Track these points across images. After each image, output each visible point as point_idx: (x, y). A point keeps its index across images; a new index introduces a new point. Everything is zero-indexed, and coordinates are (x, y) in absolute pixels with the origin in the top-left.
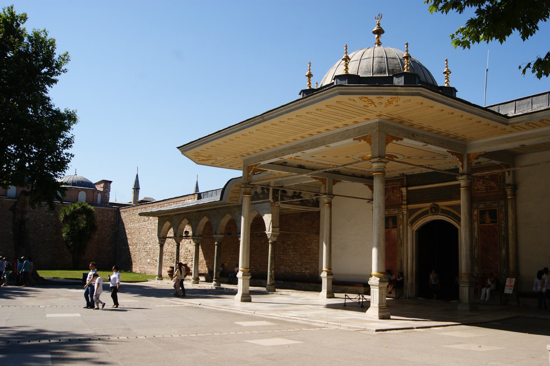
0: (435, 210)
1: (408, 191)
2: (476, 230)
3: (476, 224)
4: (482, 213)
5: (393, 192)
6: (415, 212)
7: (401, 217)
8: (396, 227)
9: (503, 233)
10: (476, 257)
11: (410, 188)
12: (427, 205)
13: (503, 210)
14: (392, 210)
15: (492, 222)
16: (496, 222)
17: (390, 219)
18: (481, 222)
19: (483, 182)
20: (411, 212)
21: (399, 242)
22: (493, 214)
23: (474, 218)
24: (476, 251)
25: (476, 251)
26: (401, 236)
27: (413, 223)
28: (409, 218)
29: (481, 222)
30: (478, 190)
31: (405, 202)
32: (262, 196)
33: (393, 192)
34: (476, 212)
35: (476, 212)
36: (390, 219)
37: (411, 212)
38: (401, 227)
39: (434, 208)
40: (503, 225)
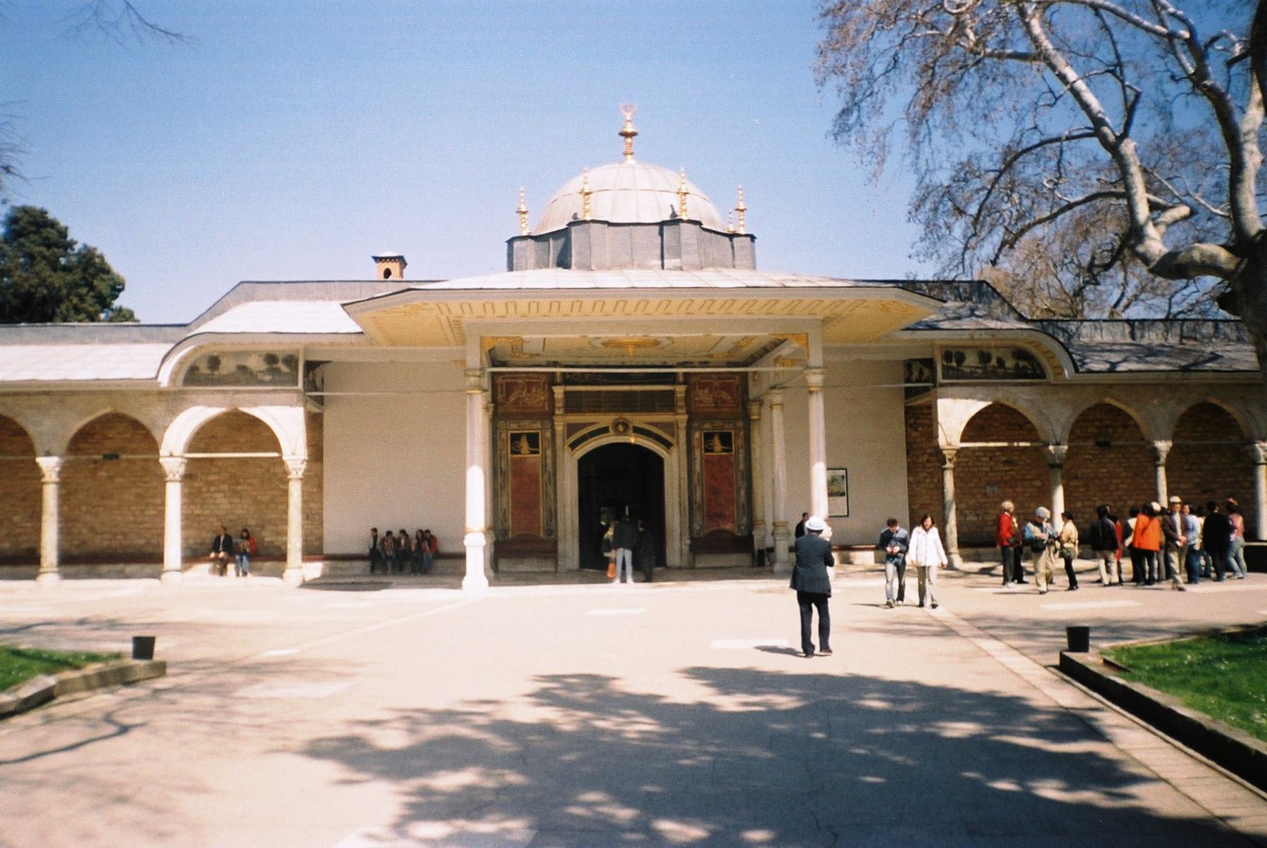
1: (566, 393)
2: (698, 460)
3: (697, 453)
4: (708, 437)
5: (529, 391)
7: (548, 435)
11: (570, 388)
12: (605, 419)
14: (526, 423)
15: (724, 451)
17: (524, 439)
18: (707, 450)
19: (710, 391)
20: (571, 429)
21: (546, 478)
22: (726, 440)
23: (696, 443)
24: (698, 494)
26: (549, 468)
27: (573, 446)
28: (569, 436)
30: (701, 402)
32: (267, 378)
33: (529, 391)
34: (697, 435)
36: (524, 439)
37: (571, 429)
38: (549, 452)
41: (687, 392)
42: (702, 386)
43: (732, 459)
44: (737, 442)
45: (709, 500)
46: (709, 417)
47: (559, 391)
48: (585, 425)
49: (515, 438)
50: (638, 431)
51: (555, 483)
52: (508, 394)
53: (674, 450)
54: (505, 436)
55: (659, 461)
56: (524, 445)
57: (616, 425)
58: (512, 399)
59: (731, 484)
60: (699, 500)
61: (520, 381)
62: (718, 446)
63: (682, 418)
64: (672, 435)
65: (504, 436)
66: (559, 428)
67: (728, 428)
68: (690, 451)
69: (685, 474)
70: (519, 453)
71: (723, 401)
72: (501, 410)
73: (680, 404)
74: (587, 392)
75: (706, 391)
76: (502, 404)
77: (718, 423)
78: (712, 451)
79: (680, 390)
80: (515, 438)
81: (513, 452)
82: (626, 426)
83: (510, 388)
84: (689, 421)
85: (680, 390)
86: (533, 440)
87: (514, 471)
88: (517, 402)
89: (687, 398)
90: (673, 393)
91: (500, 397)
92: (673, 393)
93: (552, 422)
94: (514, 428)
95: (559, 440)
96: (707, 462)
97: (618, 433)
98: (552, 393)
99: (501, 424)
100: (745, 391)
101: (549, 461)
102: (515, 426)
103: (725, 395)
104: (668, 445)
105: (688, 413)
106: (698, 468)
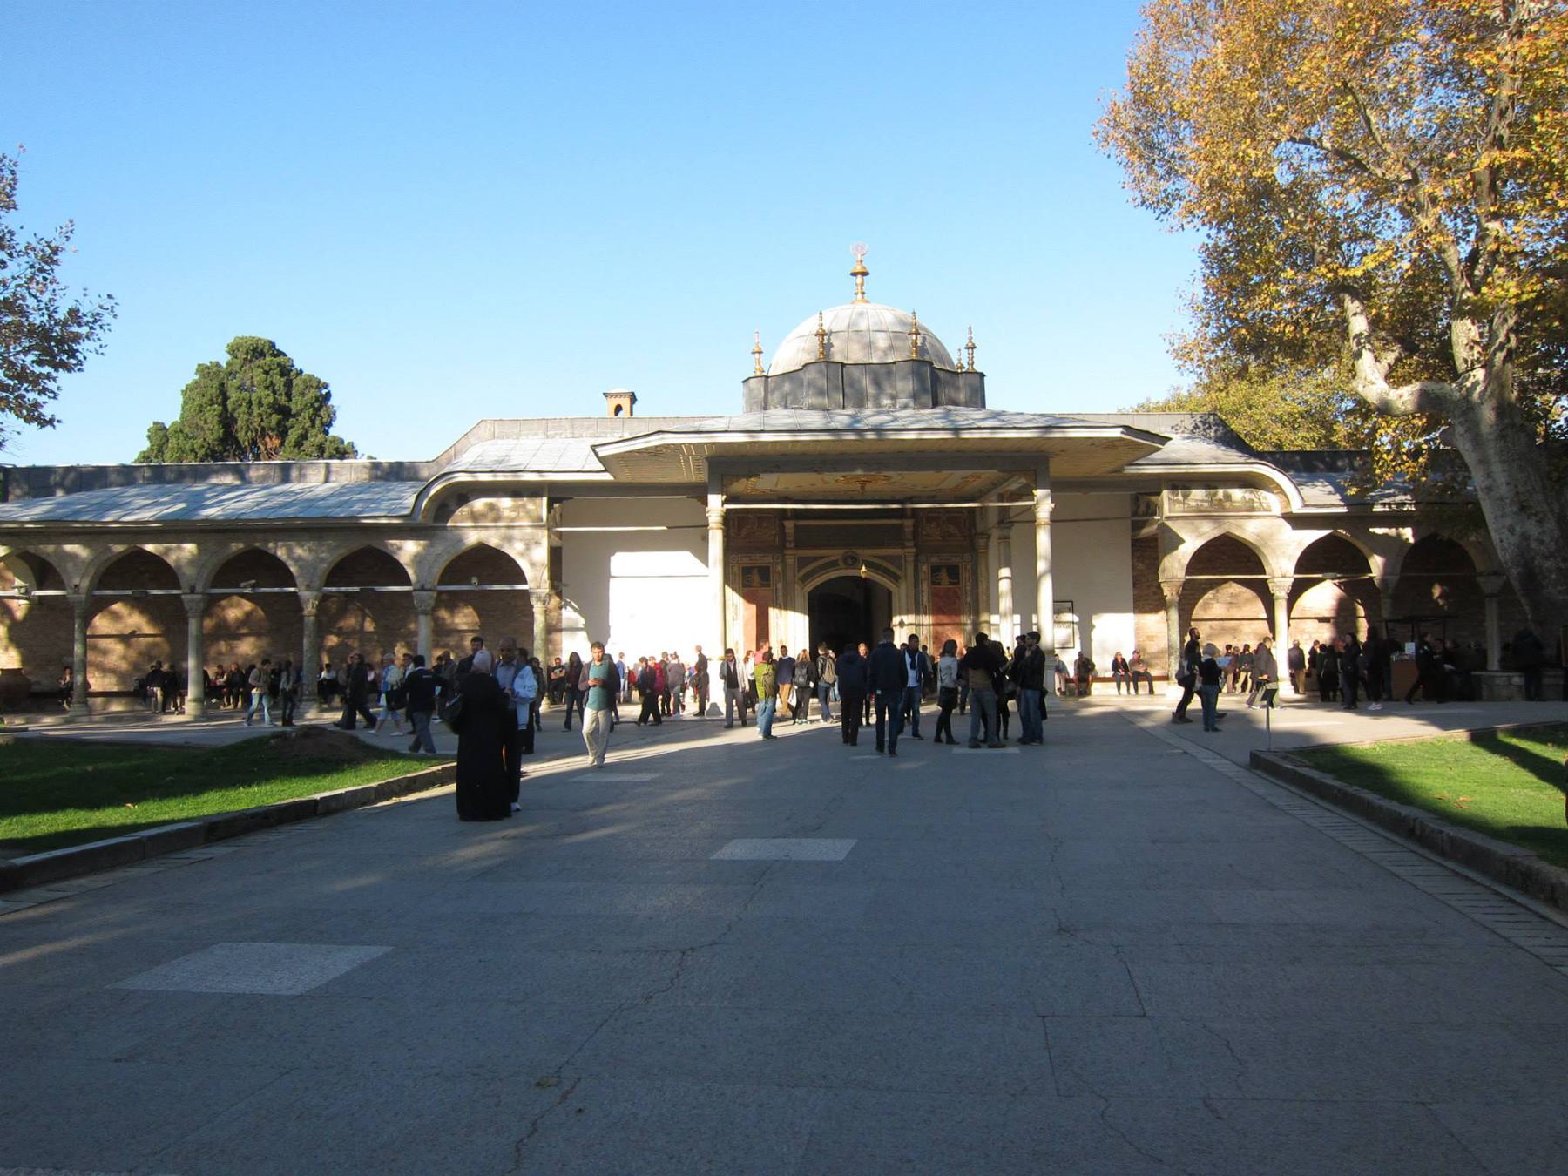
4: (935, 570)
7: (779, 568)
12: (836, 554)
22: (954, 572)
23: (922, 576)
27: (805, 579)
29: (933, 583)
34: (924, 568)
35: (924, 568)
37: (803, 562)
38: (780, 586)
41: (915, 526)
44: (965, 575)
47: (789, 525)
48: (815, 559)
53: (903, 587)
55: (890, 593)
57: (845, 559)
58: (744, 533)
66: (790, 561)
67: (955, 561)
79: (909, 523)
84: (916, 555)
85: (909, 523)
90: (901, 527)
92: (901, 527)
95: (790, 573)
97: (848, 566)
98: (783, 527)
102: (746, 560)
103: (952, 529)
104: (896, 578)
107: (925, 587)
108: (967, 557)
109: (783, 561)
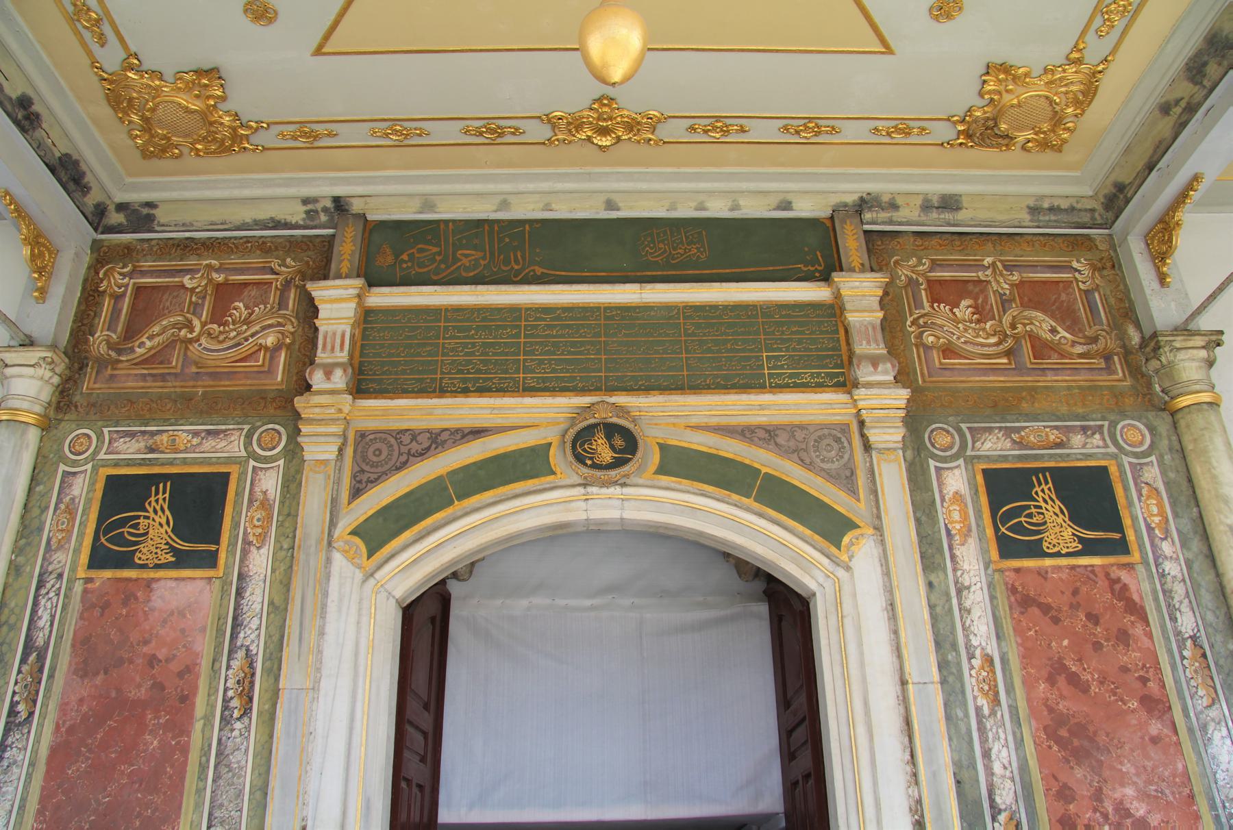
0: (608, 447)
1: (367, 317)
2: (977, 598)
4: (1005, 488)
5: (219, 315)
6: (423, 454)
7: (270, 483)
8: (210, 560)
9: (1187, 623)
10: (1006, 796)
12: (540, 416)
13: (1152, 474)
14: (183, 433)
15: (1089, 548)
16: (1121, 547)
17: (159, 500)
19: (982, 314)
21: (230, 677)
24: (1003, 755)
25: (1003, 755)
26: (254, 635)
27: (378, 533)
28: (356, 493)
29: (1007, 548)
30: (948, 351)
31: (339, 379)
33: (219, 315)
35: (956, 481)
36: (159, 500)
38: (261, 562)
39: (611, 430)
40: (1168, 566)
41: (888, 300)
42: (944, 292)
43: (1141, 586)
45: (1064, 794)
46: (999, 407)
47: (338, 304)
48: (437, 440)
49: (124, 495)
50: (681, 464)
51: (270, 718)
52: (131, 333)
53: (863, 553)
54: (85, 490)
56: (157, 525)
57: (580, 443)
58: (146, 345)
59: (1156, 705)
60: (1006, 796)
61: (187, 281)
62: (1059, 529)
63: (882, 399)
64: (847, 480)
65: (79, 488)
66: (320, 448)
67: (1085, 449)
68: (932, 553)
69: (923, 664)
70: (125, 561)
71: (1041, 348)
72: (90, 384)
73: (861, 348)
74: (458, 310)
75: (964, 309)
76: (102, 363)
77: (1037, 431)
78: (1035, 550)
79: (860, 292)
80: (124, 495)
81: (99, 559)
82: (626, 443)
83: (146, 304)
84: (915, 420)
86: (200, 506)
87: (83, 644)
88: (157, 357)
89: (891, 328)
90: (834, 310)
91: (99, 341)
93: (294, 420)
94: (128, 451)
96: (1022, 600)
98: (310, 309)
99: (74, 432)
100: (1126, 311)
101: (257, 598)
103: (1042, 324)
104: (831, 527)
105: (903, 377)
106: (981, 631)
107: (972, 561)
108: (1134, 432)
109: (294, 452)
